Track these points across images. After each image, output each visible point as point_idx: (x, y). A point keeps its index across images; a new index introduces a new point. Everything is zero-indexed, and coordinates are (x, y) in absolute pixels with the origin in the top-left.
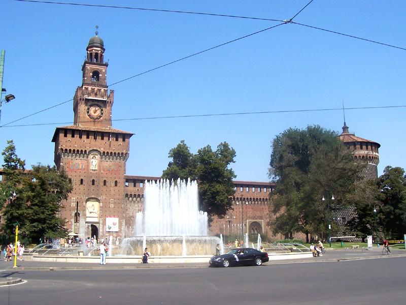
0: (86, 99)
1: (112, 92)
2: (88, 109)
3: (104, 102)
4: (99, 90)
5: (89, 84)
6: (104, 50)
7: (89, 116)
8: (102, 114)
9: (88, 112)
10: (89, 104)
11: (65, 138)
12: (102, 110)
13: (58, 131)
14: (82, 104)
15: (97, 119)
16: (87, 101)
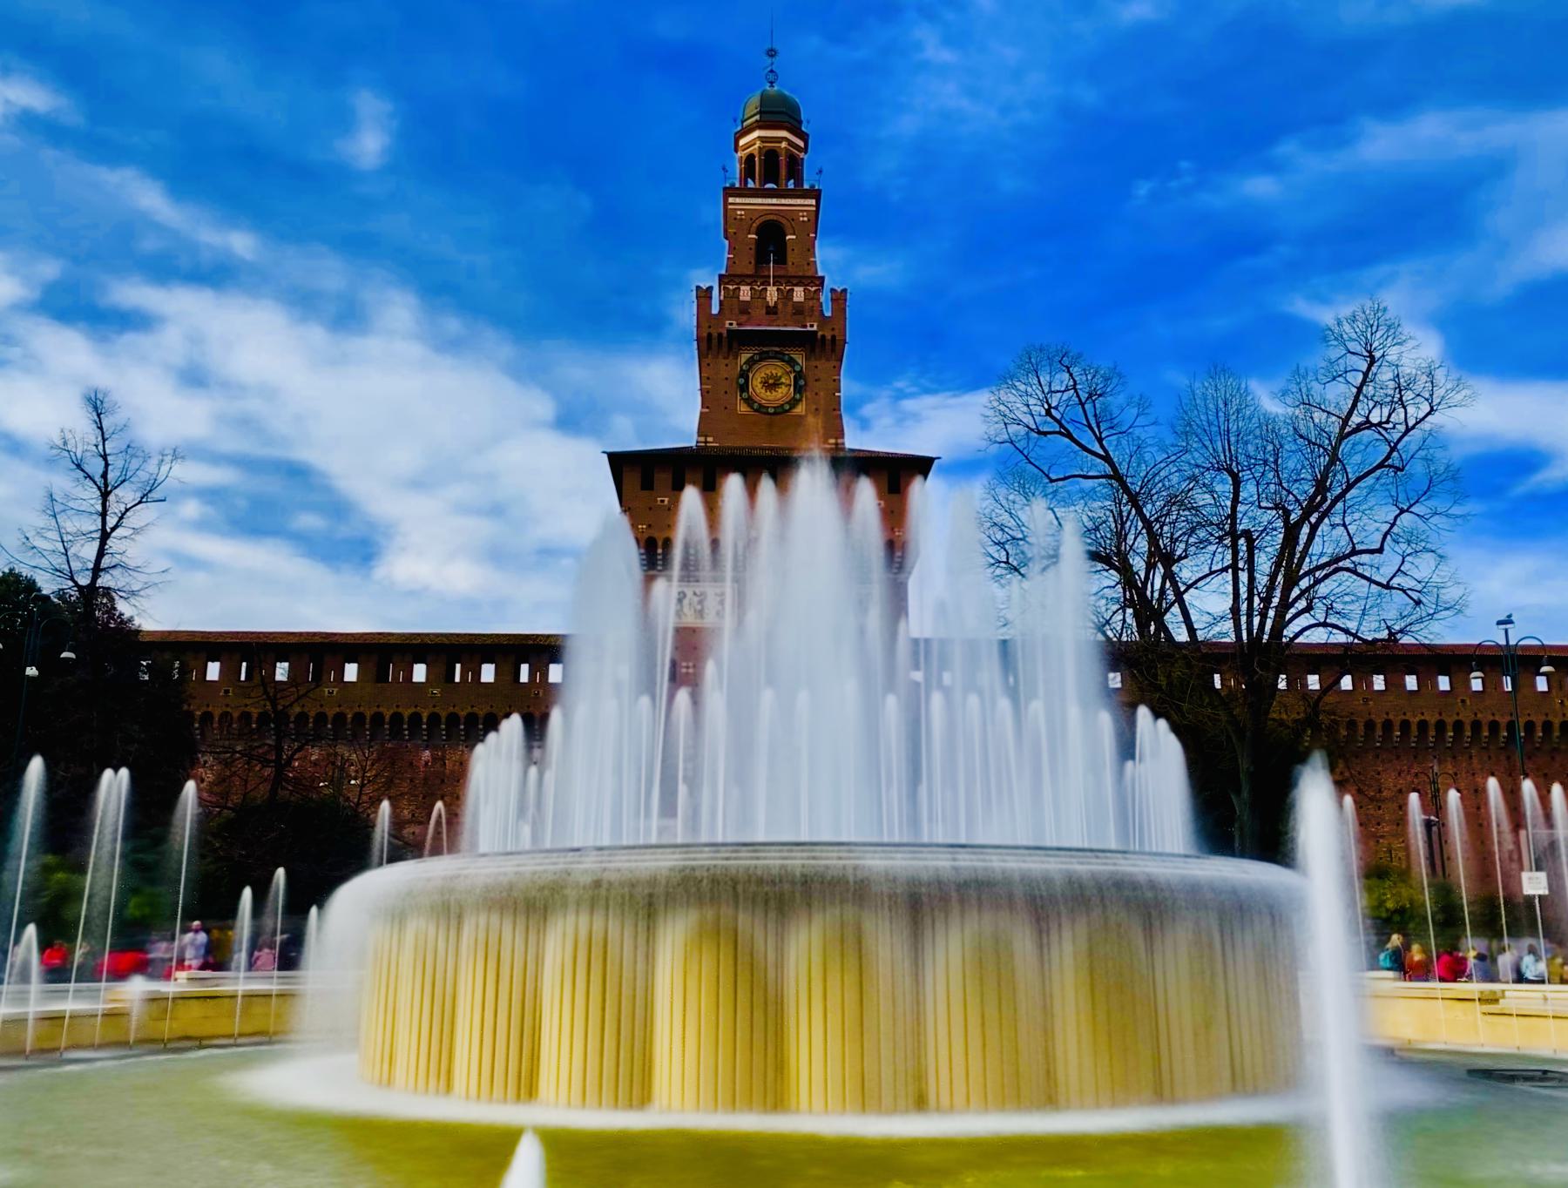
0: (729, 331)
1: (839, 298)
2: (744, 374)
3: (808, 342)
4: (786, 296)
5: (741, 279)
6: (804, 136)
7: (749, 401)
8: (799, 389)
9: (744, 388)
10: (745, 357)
11: (646, 493)
12: (799, 376)
13: (621, 463)
14: (716, 357)
15: (780, 411)
16: (735, 345)
